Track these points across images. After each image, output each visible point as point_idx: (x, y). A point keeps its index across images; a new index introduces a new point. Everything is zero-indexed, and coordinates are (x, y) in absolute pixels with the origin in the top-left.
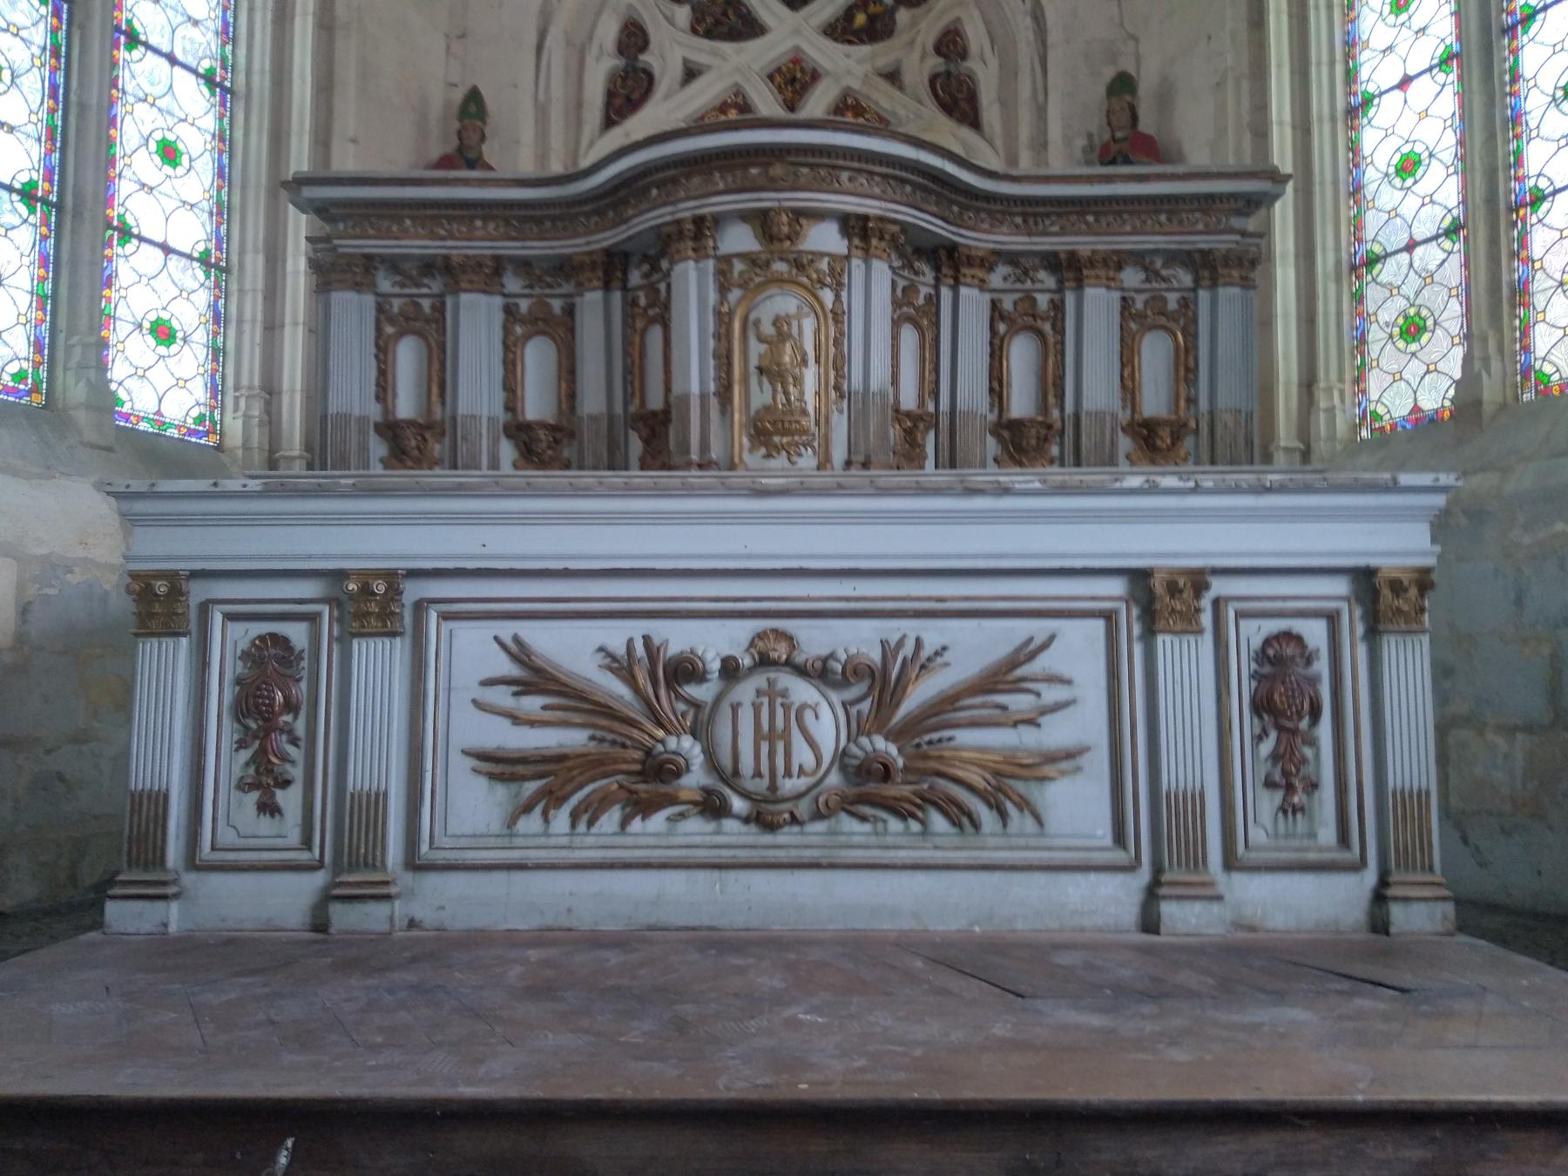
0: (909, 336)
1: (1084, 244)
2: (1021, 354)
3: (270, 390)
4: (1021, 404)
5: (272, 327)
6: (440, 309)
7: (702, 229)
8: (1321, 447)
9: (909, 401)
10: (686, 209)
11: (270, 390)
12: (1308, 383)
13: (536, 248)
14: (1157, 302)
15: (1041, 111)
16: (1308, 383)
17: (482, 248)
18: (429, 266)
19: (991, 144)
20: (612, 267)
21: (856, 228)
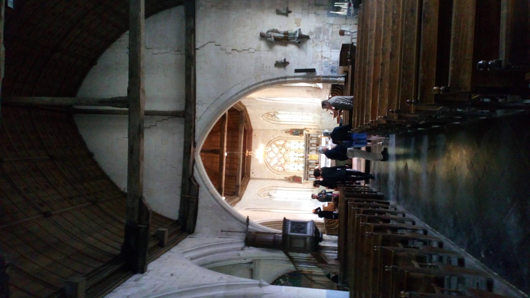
0: (312, 151)
1: (308, 142)
2: (313, 145)
3: (307, 191)
4: (315, 145)
5: (303, 191)
6: (309, 174)
7: (308, 161)
8: (314, 122)
9: (315, 151)
10: (307, 161)
11: (307, 191)
12: (309, 122)
13: (307, 169)
14: (311, 138)
15: (285, 137)
16: (309, 122)
17: (306, 172)
18: (307, 175)
19: (286, 141)
20: (308, 166)
21: (308, 153)
